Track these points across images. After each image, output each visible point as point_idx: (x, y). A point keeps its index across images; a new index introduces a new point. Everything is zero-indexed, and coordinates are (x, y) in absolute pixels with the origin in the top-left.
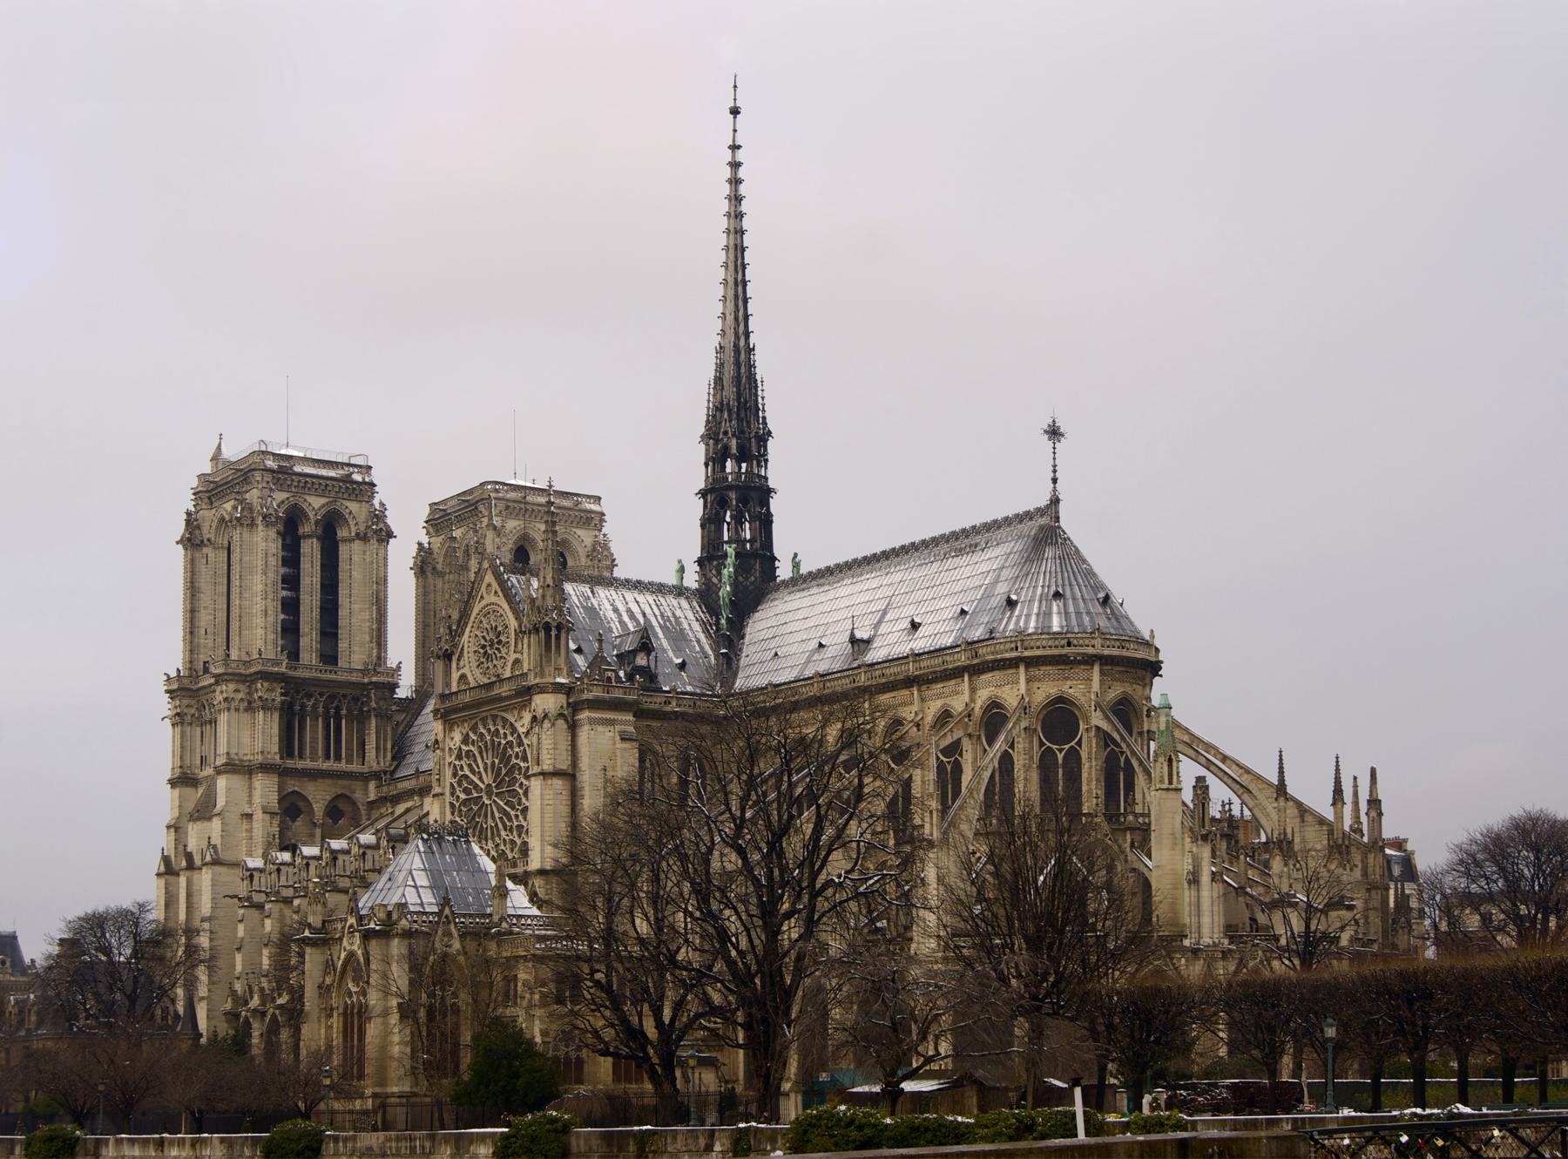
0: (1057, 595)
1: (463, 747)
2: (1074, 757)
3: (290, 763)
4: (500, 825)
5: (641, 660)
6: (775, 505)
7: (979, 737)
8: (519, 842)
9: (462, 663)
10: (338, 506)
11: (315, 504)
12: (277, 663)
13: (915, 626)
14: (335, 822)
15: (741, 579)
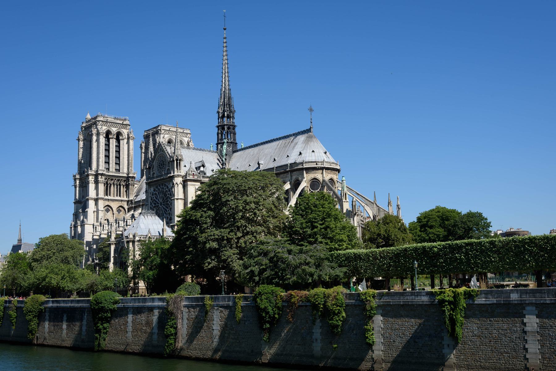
0: (313, 151)
1: (154, 192)
3: (106, 197)
4: (164, 213)
6: (237, 129)
7: (293, 189)
8: (169, 217)
9: (153, 170)
10: (120, 130)
11: (114, 130)
12: (104, 171)
14: (119, 213)
15: (228, 148)
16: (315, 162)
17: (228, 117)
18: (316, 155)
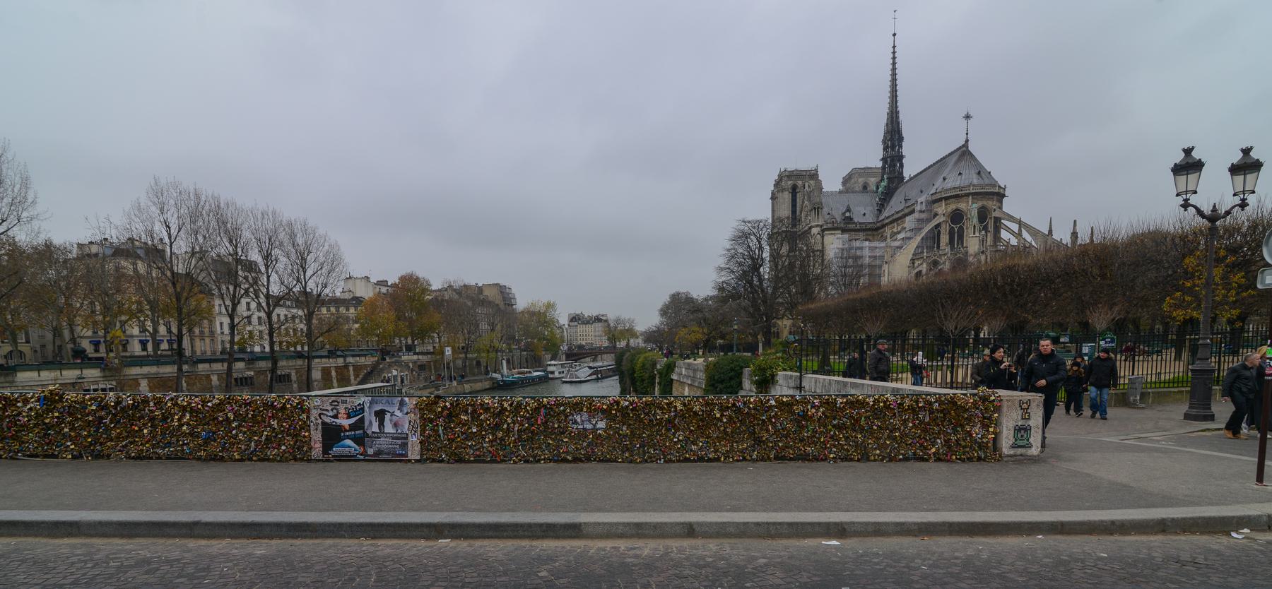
0: (960, 174)
2: (961, 229)
5: (848, 214)
6: (904, 161)
11: (800, 183)
13: (921, 192)
16: (957, 188)
17: (893, 147)
18: (963, 178)
